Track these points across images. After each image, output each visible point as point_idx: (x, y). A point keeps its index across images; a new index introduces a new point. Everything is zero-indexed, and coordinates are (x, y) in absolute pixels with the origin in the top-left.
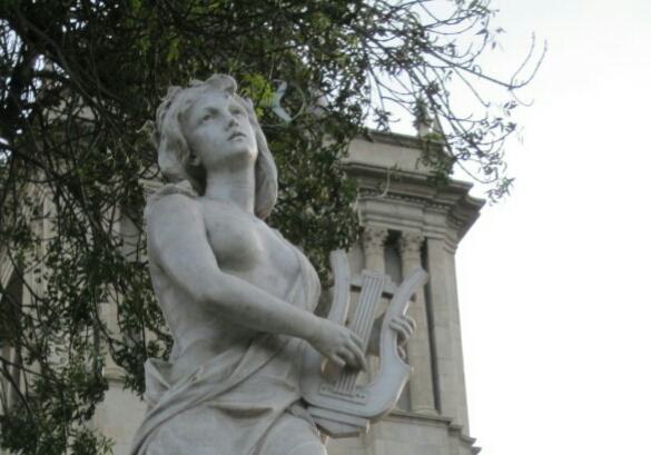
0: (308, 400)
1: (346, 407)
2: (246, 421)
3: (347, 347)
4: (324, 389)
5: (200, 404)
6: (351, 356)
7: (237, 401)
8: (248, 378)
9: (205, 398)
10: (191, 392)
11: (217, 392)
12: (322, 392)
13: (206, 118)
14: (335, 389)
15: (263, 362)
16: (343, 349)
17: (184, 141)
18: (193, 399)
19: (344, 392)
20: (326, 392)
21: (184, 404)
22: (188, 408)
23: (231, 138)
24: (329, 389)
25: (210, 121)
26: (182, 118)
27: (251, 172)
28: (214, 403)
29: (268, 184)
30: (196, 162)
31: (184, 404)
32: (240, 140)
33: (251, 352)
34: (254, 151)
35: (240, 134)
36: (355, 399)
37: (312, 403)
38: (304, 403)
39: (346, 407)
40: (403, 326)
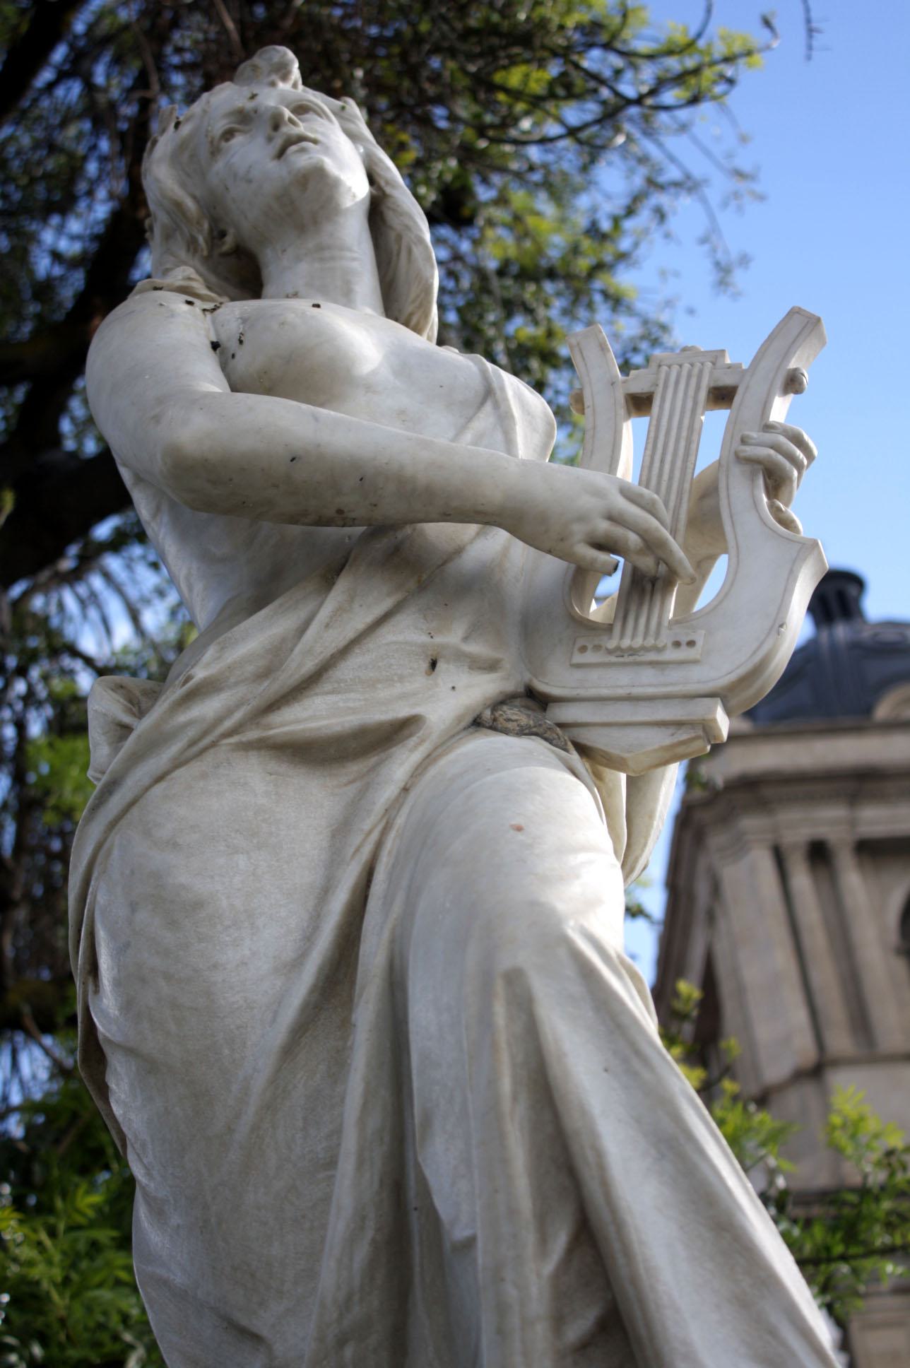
0: (542, 687)
1: (646, 681)
2: (354, 768)
3: (612, 518)
4: (583, 649)
5: (214, 744)
6: (633, 539)
7: (318, 715)
8: (344, 652)
9: (228, 724)
10: (182, 718)
11: (255, 703)
12: (579, 658)
13: (228, 134)
14: (612, 644)
15: (387, 604)
16: (603, 526)
17: (190, 204)
18: (191, 733)
19: (639, 642)
20: (589, 657)
21: (174, 749)
22: (178, 763)
23: (281, 153)
24: (597, 648)
25: (238, 140)
26: (185, 156)
27: (353, 232)
28: (252, 734)
29: (410, 252)
30: (229, 242)
31: (174, 749)
32: (303, 150)
33: (342, 585)
34: (356, 187)
35: (302, 139)
36: (671, 655)
37: (555, 691)
38: (536, 700)
39: (646, 681)
40: (777, 448)
